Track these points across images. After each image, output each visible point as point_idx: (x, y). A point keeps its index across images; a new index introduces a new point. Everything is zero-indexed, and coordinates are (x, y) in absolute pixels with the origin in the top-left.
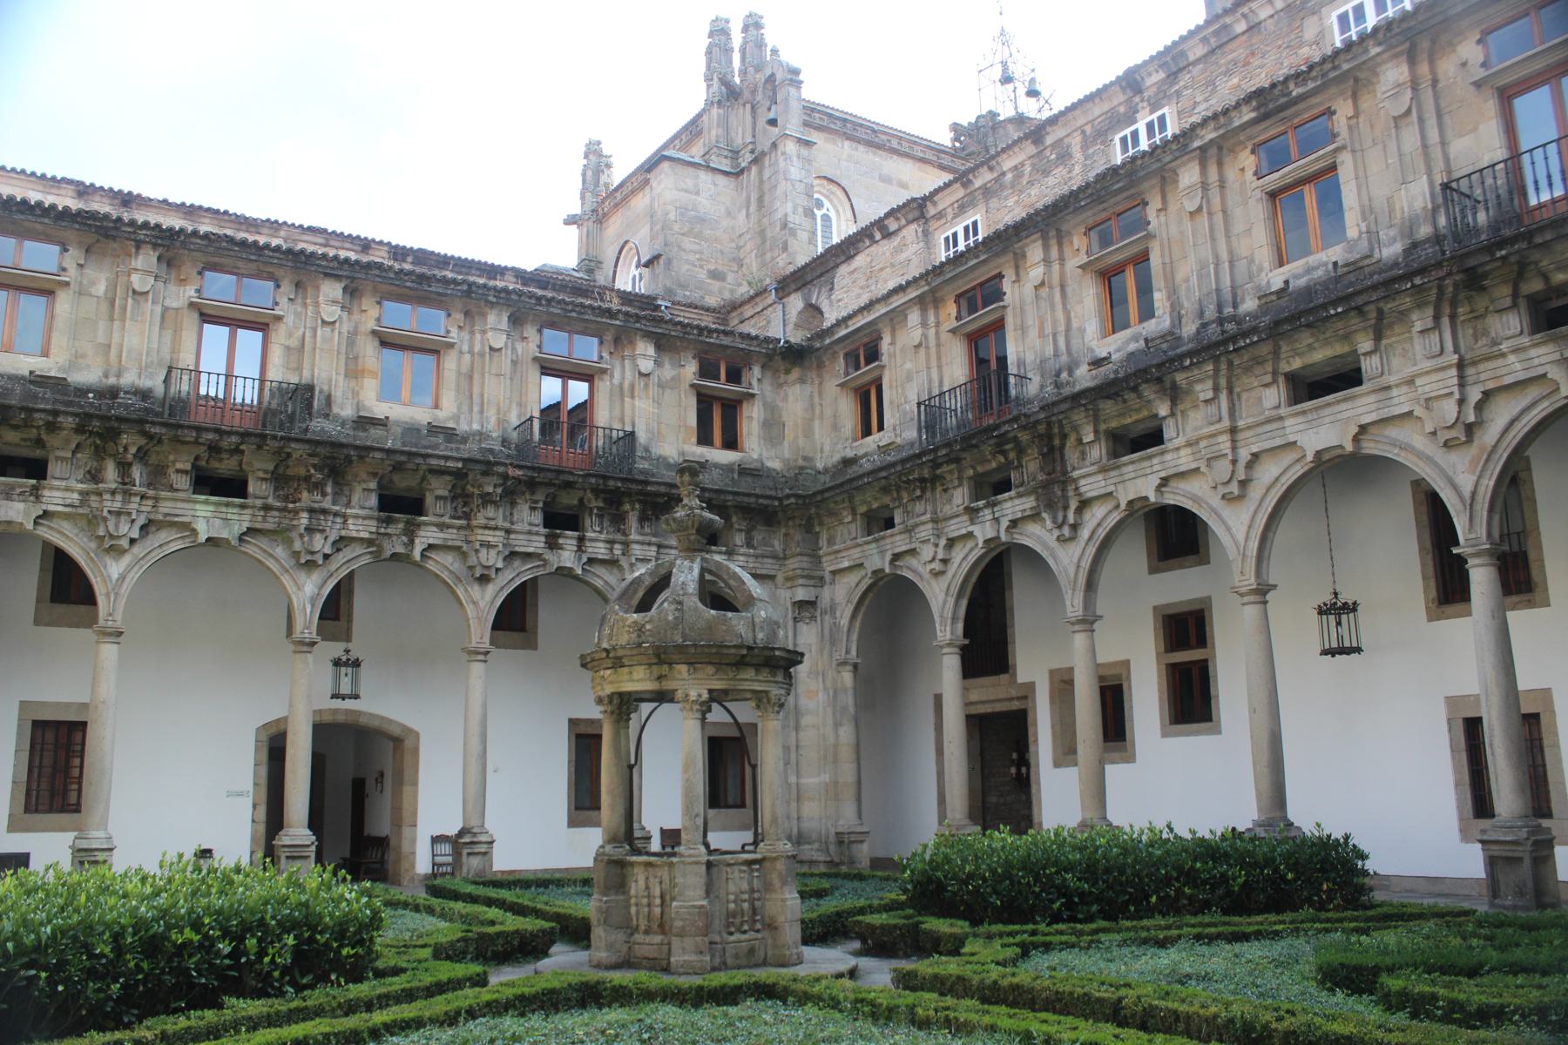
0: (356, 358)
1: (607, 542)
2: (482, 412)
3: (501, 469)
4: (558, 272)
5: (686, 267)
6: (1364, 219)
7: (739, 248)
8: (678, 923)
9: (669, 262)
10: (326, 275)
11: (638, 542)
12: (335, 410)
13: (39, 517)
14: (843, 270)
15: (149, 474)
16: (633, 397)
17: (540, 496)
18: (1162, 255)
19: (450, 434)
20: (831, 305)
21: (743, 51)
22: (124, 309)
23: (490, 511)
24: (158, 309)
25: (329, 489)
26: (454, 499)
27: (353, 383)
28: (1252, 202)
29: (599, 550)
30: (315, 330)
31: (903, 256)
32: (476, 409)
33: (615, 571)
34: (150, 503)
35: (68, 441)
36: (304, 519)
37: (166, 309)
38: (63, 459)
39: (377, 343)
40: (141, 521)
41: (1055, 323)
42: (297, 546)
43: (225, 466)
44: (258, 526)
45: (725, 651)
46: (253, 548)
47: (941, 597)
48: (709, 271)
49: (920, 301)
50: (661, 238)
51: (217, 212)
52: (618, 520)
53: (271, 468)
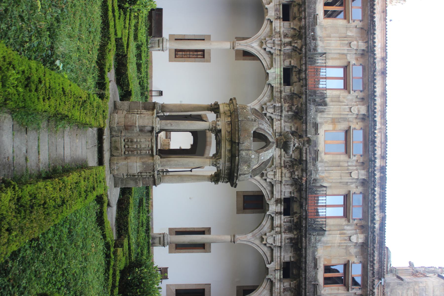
0: (339, 122)
1: (280, 225)
3: (304, 175)
4: (388, 257)
5: (400, 292)
8: (130, 116)
9: (401, 285)
10: (368, 106)
11: (281, 237)
12: (319, 115)
13: (270, 20)
15: (288, 53)
16: (340, 234)
17: (296, 195)
19: (315, 159)
22: (344, 40)
23: (288, 175)
24: (346, 52)
25: (290, 113)
26: (291, 161)
27: (330, 121)
29: (277, 222)
30: (347, 105)
32: (327, 168)
33: (269, 230)
34: (279, 53)
35: (296, 25)
36: (278, 105)
37: (346, 55)
38: (290, 25)
39: (346, 129)
40: (272, 51)
42: (268, 104)
43: (294, 78)
44: (274, 90)
45: (237, 132)
46: (267, 89)
50: (410, 281)
51: (386, 103)
52: (290, 230)
53: (295, 92)
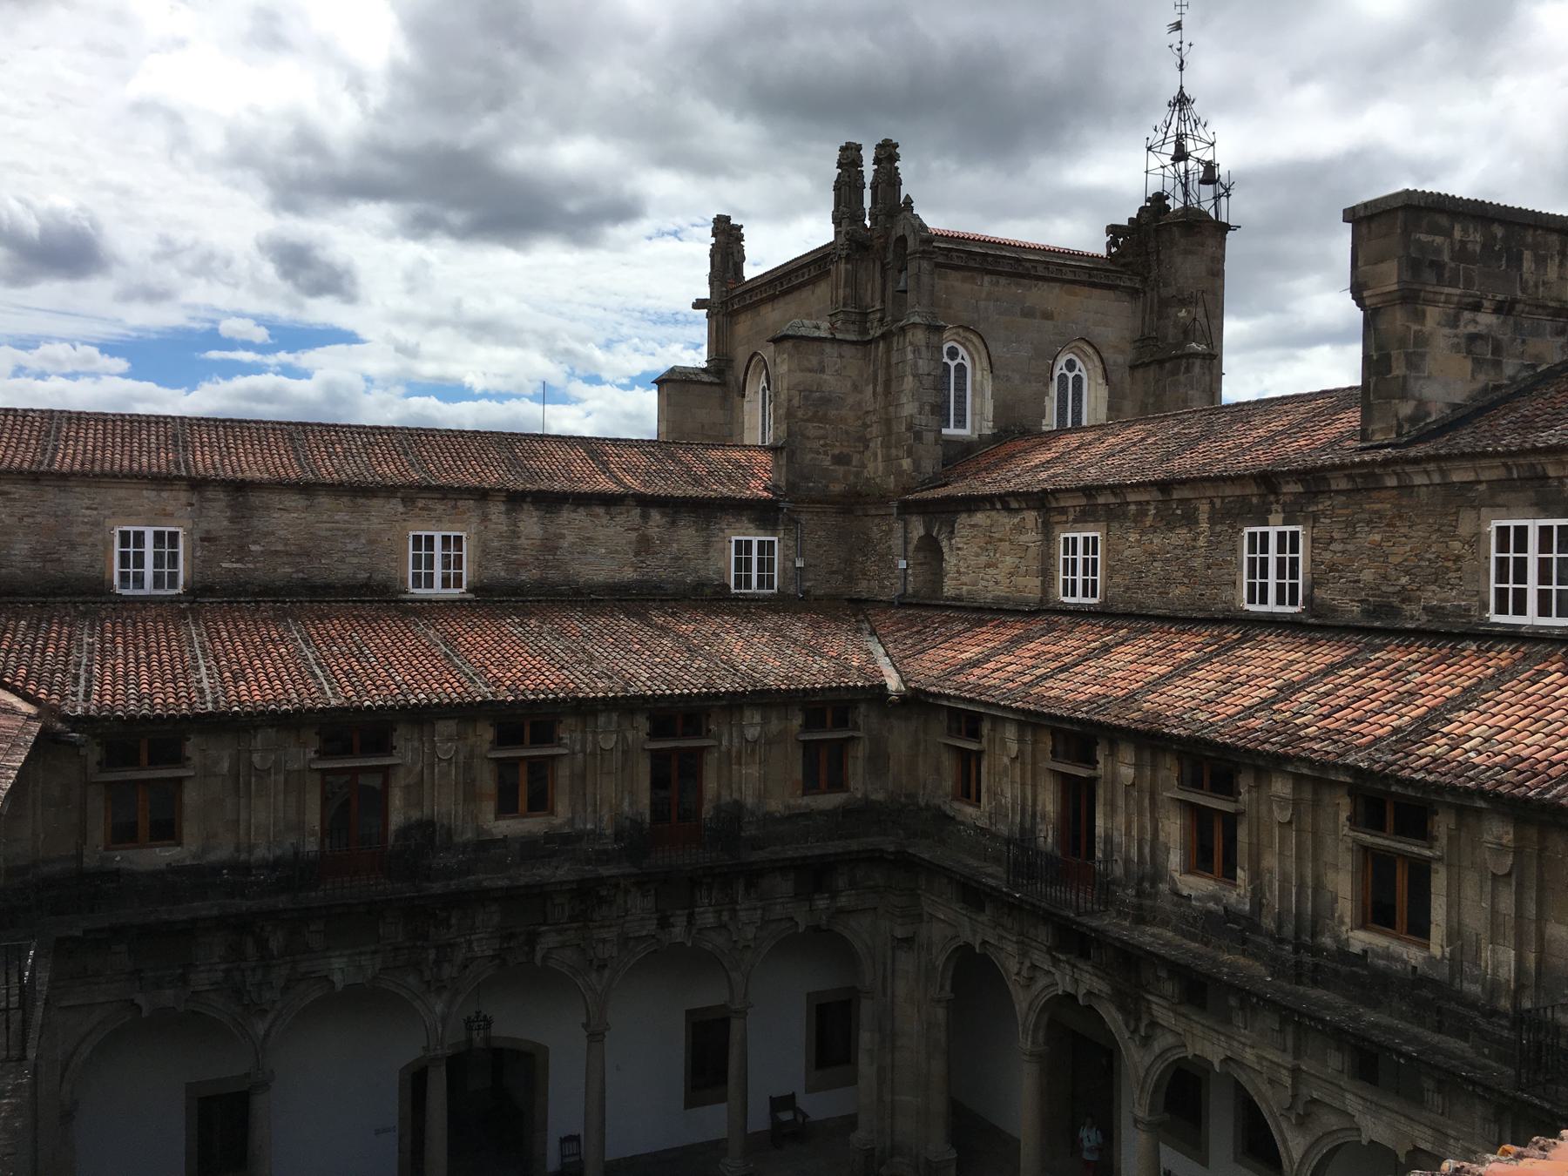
2: (595, 811)
5: (809, 457)
6: (1450, 942)
7: (865, 426)
14: (963, 519)
18: (1250, 834)
20: (951, 549)
21: (874, 187)
28: (1341, 847)
31: (1023, 538)
41: (1141, 829)
47: (1025, 1005)
48: (833, 456)
49: (1019, 722)
